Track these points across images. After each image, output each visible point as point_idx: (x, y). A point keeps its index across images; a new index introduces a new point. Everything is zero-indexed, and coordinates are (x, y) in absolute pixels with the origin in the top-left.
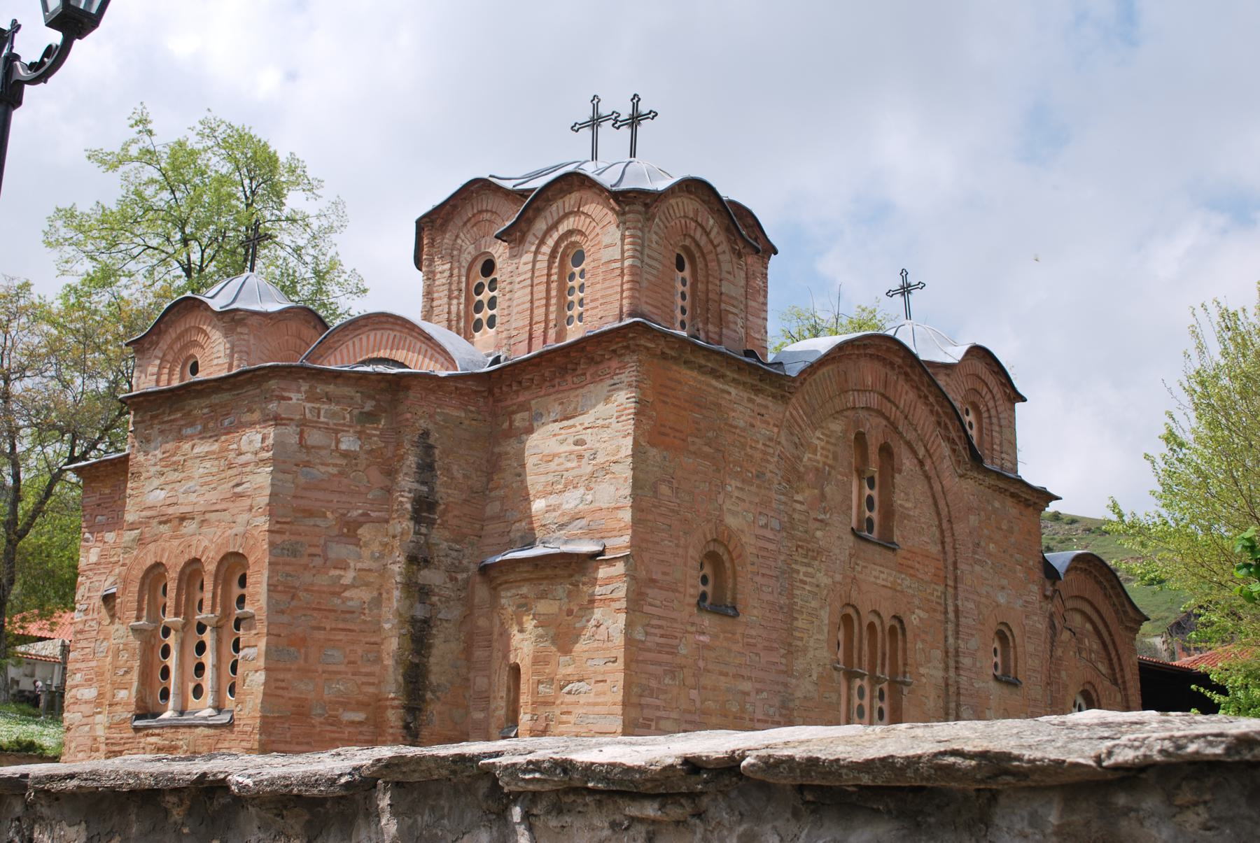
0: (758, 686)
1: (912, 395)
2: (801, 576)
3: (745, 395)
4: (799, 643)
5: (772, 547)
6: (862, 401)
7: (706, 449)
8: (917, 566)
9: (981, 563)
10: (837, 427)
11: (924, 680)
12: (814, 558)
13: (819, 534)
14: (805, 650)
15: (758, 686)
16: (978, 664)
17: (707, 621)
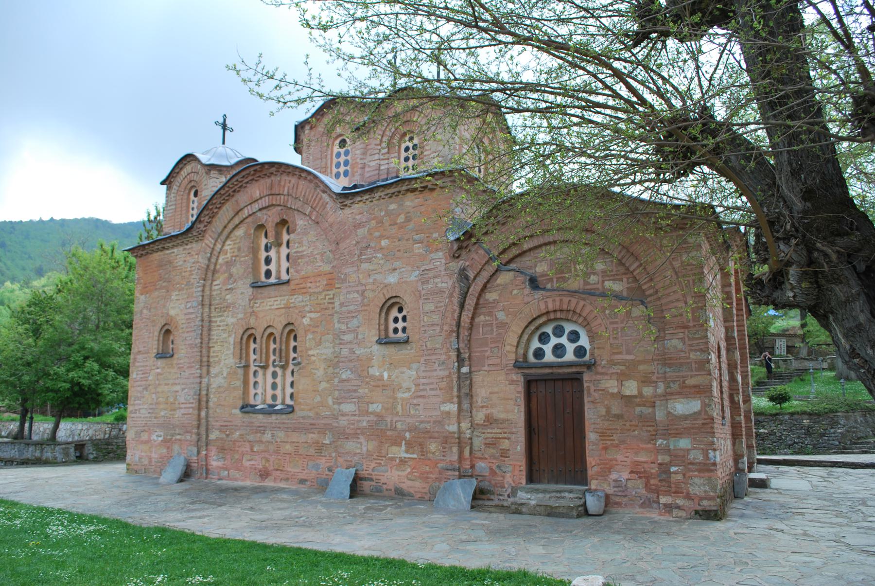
0: (183, 387)
1: (294, 180)
2: (218, 323)
3: (181, 248)
4: (216, 359)
5: (193, 316)
6: (256, 207)
7: (164, 284)
8: (309, 285)
9: (369, 261)
10: (240, 232)
11: (313, 358)
12: (225, 311)
13: (228, 297)
14: (219, 362)
15: (183, 387)
16: (360, 337)
17: (160, 363)
